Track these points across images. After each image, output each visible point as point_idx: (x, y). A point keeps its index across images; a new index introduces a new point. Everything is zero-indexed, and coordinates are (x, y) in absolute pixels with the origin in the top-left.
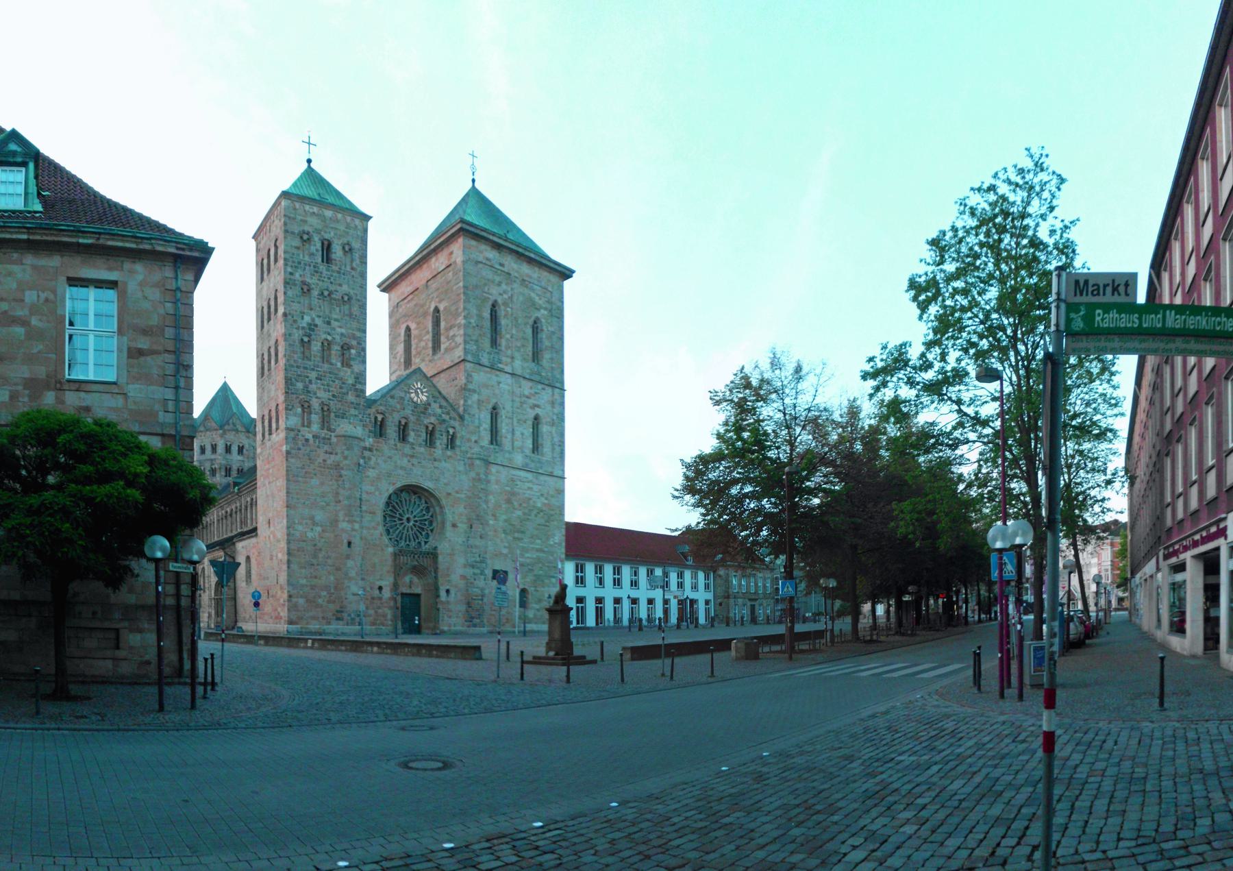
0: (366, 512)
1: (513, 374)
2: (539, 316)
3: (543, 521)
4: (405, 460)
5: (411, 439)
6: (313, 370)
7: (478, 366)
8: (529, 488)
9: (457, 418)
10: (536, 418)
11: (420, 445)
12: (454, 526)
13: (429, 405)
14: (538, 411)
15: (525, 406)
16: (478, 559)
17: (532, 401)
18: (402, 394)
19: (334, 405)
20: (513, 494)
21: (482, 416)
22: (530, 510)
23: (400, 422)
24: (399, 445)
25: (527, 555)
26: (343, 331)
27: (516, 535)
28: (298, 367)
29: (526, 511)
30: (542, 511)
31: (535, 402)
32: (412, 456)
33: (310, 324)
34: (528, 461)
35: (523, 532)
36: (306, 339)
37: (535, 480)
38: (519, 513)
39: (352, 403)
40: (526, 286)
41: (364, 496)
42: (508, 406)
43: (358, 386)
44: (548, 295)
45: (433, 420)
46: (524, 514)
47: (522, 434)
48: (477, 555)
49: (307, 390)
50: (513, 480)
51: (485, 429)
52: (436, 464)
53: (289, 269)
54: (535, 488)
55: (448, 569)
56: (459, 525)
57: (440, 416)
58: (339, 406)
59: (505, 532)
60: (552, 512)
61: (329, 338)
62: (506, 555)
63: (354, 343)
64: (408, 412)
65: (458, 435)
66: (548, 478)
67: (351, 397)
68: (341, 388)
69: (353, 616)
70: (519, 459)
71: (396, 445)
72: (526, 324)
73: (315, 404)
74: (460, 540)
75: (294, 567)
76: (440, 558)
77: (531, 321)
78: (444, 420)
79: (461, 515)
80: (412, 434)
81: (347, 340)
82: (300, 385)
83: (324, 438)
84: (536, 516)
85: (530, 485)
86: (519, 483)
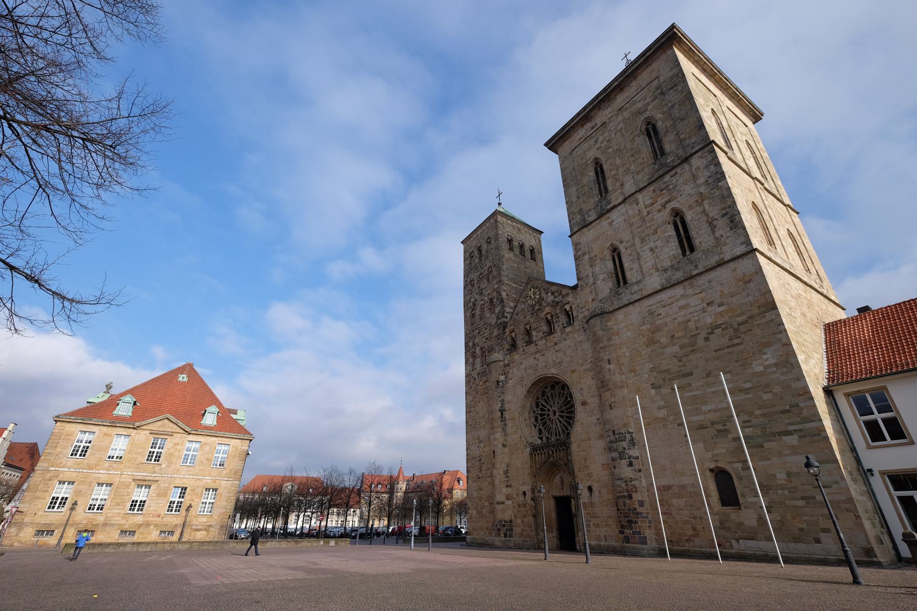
0: (509, 419)
2: (648, 114)
3: (725, 341)
7: (585, 230)
8: (681, 308)
9: (570, 291)
12: (584, 403)
13: (543, 299)
14: (670, 206)
16: (612, 438)
18: (523, 306)
25: (705, 408)
29: (686, 341)
30: (718, 327)
31: (661, 202)
32: (536, 353)
35: (690, 374)
37: (689, 292)
38: (676, 349)
40: (626, 109)
41: (507, 406)
42: (626, 237)
45: (548, 310)
46: (681, 347)
48: (611, 433)
50: (651, 313)
52: (557, 347)
54: (693, 301)
55: (585, 460)
56: (589, 401)
57: (553, 301)
59: (653, 386)
62: (664, 419)
70: (654, 282)
71: (524, 350)
74: (594, 419)
75: (470, 482)
78: (557, 303)
79: (590, 388)
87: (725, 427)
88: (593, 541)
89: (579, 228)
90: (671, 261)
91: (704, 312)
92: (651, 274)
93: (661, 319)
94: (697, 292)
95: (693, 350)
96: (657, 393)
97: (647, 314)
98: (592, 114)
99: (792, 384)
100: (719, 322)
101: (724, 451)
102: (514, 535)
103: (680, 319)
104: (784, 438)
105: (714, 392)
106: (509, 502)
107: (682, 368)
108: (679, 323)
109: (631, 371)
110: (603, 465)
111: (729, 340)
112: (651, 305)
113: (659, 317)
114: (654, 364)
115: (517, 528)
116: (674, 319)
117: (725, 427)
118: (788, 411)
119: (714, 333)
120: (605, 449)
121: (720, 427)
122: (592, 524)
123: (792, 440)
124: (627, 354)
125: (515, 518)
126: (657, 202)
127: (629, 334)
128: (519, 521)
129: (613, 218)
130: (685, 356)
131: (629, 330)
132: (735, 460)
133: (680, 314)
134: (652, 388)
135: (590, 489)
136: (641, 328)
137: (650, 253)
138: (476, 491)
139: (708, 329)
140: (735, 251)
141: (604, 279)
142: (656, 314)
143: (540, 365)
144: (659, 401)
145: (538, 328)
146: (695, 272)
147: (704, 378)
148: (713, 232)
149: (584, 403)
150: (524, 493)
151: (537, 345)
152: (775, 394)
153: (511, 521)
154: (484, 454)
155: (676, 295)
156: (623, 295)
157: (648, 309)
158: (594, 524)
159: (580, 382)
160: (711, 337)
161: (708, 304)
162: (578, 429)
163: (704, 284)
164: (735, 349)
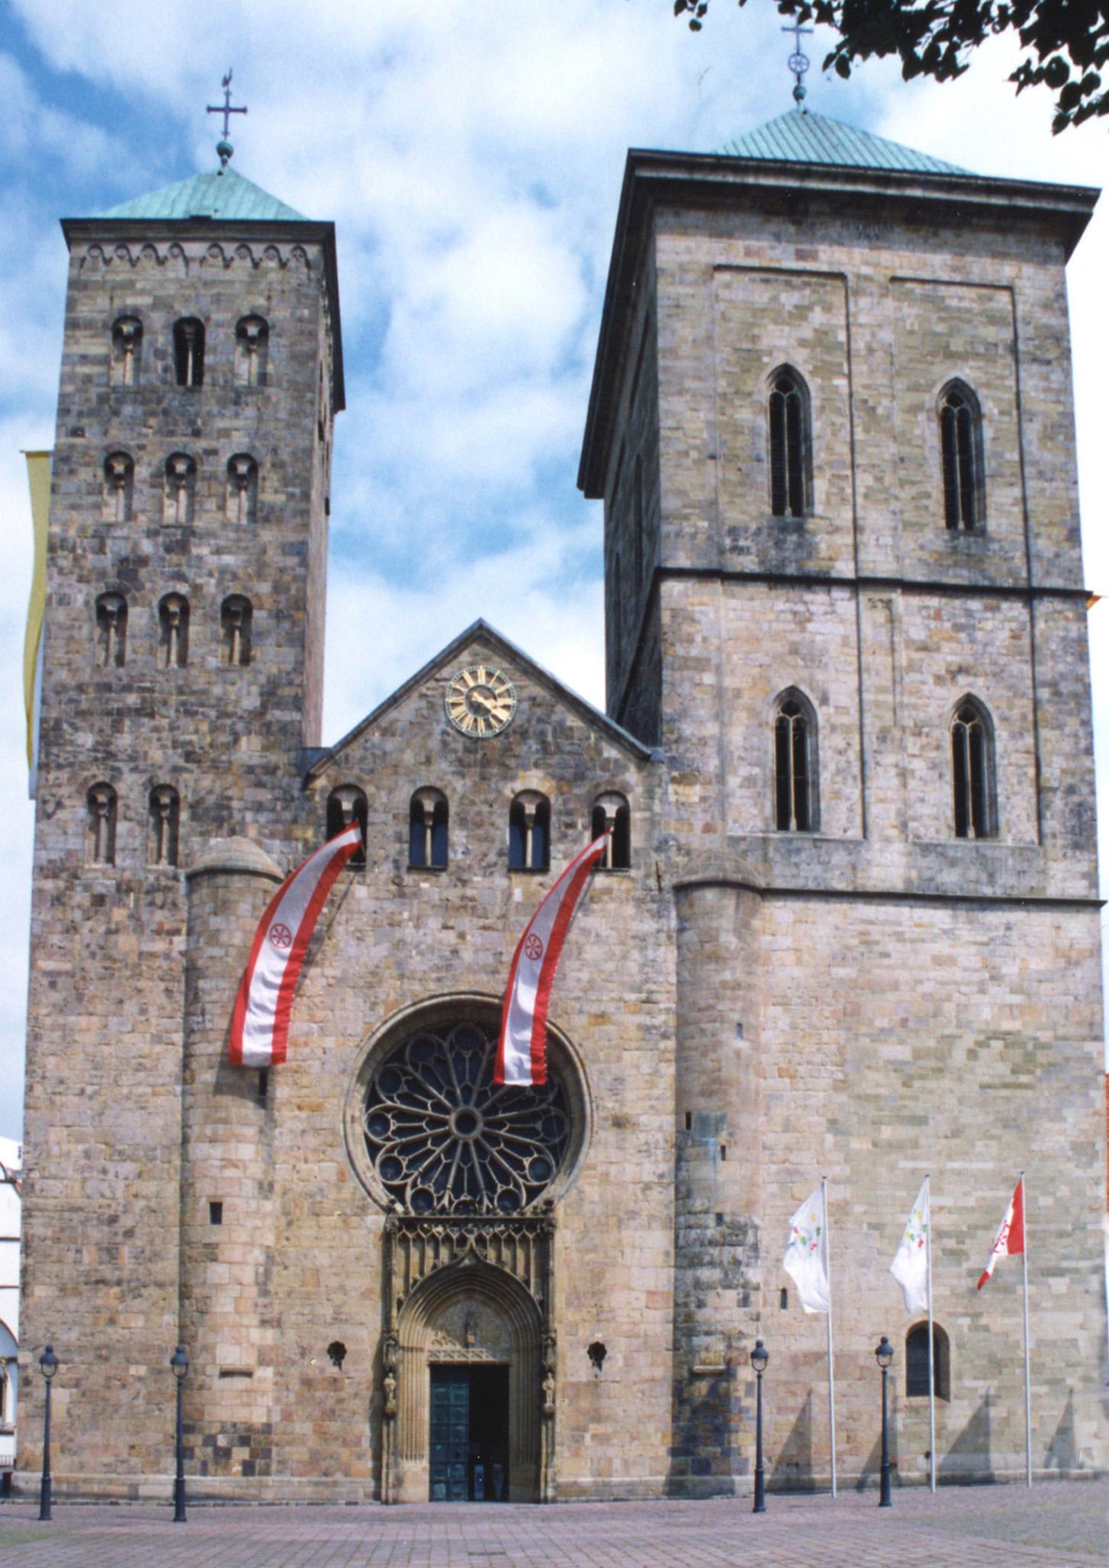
1: (858, 584)
3: (1003, 1069)
4: (434, 923)
5: (456, 856)
6: (127, 689)
8: (939, 961)
10: (970, 709)
11: (488, 870)
12: (619, 1123)
15: (911, 678)
17: (949, 655)
19: (194, 784)
20: (875, 988)
21: (736, 736)
22: (950, 1039)
23: (416, 806)
24: (409, 879)
26: (228, 559)
27: (886, 1132)
28: (81, 688)
31: (949, 658)
33: (124, 561)
34: (931, 860)
35: (920, 1121)
36: (112, 607)
38: (903, 1053)
39: (250, 770)
40: (908, 296)
43: (276, 715)
44: (1004, 297)
46: (918, 1054)
47: (904, 774)
49: (105, 753)
51: (749, 782)
53: (71, 421)
56: (643, 1119)
58: (207, 782)
60: (1045, 1036)
61: (183, 589)
63: (264, 588)
64: (442, 773)
65: (636, 816)
66: (1017, 916)
67: (249, 749)
68: (214, 729)
69: (222, 1441)
72: (915, 409)
73: (131, 788)
76: (563, 1240)
77: (934, 399)
80: (457, 836)
81: (234, 589)
82: (86, 739)
83: (152, 890)
84: (972, 1054)
85: (943, 947)
86: (891, 946)
87: (961, 1246)
88: (584, 1475)
89: (701, 564)
90: (938, 832)
91: (982, 991)
92: (887, 840)
93: (889, 967)
94: (979, 939)
95: (940, 1070)
96: (836, 1144)
97: (855, 942)
98: (813, 208)
99: (1088, 1188)
100: (1007, 1025)
101: (948, 1292)
102: (274, 1467)
103: (928, 987)
104: (1052, 1281)
105: (959, 1173)
106: (266, 1373)
107: (908, 1103)
108: (926, 997)
109: (782, 1073)
110: (651, 1293)
111: (1014, 1072)
112: (872, 922)
113: (886, 961)
114: (846, 1076)
115: (287, 1449)
116: (920, 982)
117: (961, 1246)
118: (1068, 1235)
119: (989, 1046)
120: (667, 1254)
121: (951, 1243)
122: (588, 1437)
123: (1059, 1285)
124: (784, 1022)
125: (287, 1416)
126: (938, 649)
127: (797, 972)
128: (303, 1427)
129: (813, 608)
130: (922, 1077)
131: (799, 962)
132: (959, 1310)
133: (932, 974)
134: (828, 1130)
135: (597, 1352)
136: (834, 971)
137: (895, 782)
138: (81, 1324)
139: (980, 1032)
140: (1068, 884)
141: (749, 782)
142: (877, 948)
143: (467, 955)
144: (838, 1163)
145: (479, 825)
146: (988, 891)
147: (946, 1137)
148: (1040, 817)
149: (619, 1123)
150: (337, 1351)
151: (464, 883)
152: (1058, 1201)
153: (268, 1428)
154: (142, 1203)
155: (932, 925)
156: (804, 856)
157: (861, 927)
158: (594, 1436)
159: (619, 1059)
160: (983, 1053)
161: (993, 978)
162: (587, 1189)
163: (996, 928)
164: (1019, 1093)
